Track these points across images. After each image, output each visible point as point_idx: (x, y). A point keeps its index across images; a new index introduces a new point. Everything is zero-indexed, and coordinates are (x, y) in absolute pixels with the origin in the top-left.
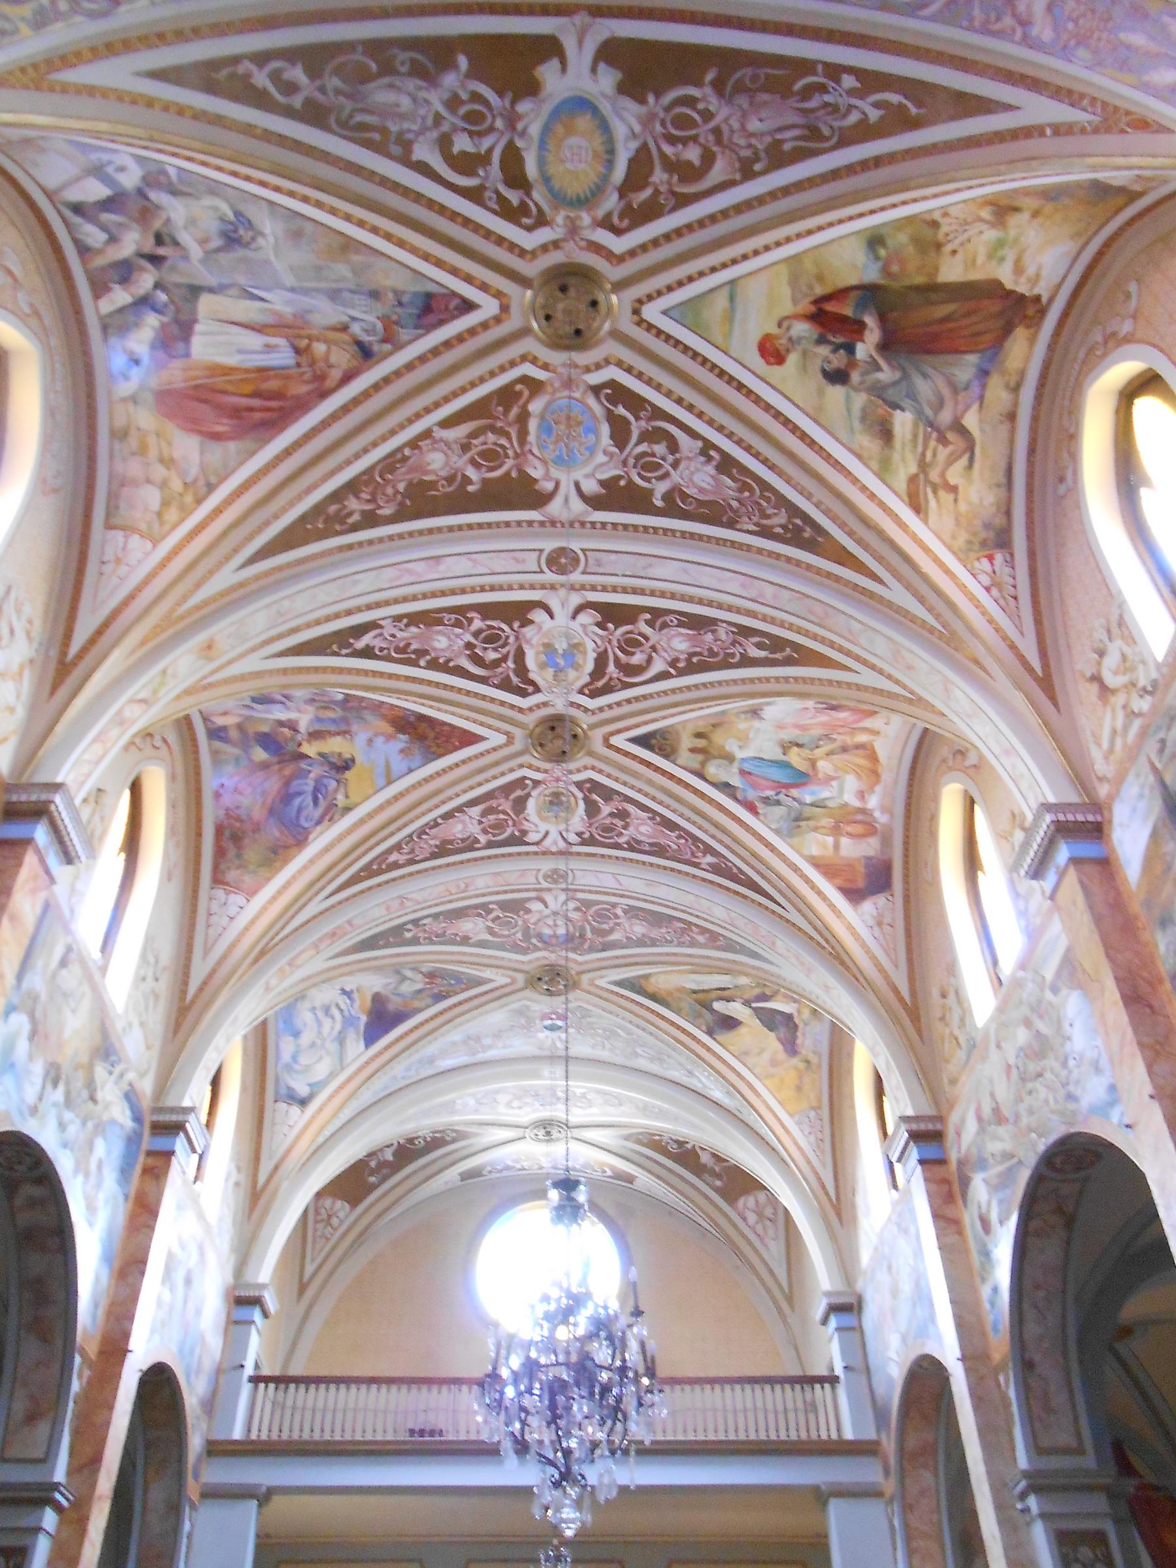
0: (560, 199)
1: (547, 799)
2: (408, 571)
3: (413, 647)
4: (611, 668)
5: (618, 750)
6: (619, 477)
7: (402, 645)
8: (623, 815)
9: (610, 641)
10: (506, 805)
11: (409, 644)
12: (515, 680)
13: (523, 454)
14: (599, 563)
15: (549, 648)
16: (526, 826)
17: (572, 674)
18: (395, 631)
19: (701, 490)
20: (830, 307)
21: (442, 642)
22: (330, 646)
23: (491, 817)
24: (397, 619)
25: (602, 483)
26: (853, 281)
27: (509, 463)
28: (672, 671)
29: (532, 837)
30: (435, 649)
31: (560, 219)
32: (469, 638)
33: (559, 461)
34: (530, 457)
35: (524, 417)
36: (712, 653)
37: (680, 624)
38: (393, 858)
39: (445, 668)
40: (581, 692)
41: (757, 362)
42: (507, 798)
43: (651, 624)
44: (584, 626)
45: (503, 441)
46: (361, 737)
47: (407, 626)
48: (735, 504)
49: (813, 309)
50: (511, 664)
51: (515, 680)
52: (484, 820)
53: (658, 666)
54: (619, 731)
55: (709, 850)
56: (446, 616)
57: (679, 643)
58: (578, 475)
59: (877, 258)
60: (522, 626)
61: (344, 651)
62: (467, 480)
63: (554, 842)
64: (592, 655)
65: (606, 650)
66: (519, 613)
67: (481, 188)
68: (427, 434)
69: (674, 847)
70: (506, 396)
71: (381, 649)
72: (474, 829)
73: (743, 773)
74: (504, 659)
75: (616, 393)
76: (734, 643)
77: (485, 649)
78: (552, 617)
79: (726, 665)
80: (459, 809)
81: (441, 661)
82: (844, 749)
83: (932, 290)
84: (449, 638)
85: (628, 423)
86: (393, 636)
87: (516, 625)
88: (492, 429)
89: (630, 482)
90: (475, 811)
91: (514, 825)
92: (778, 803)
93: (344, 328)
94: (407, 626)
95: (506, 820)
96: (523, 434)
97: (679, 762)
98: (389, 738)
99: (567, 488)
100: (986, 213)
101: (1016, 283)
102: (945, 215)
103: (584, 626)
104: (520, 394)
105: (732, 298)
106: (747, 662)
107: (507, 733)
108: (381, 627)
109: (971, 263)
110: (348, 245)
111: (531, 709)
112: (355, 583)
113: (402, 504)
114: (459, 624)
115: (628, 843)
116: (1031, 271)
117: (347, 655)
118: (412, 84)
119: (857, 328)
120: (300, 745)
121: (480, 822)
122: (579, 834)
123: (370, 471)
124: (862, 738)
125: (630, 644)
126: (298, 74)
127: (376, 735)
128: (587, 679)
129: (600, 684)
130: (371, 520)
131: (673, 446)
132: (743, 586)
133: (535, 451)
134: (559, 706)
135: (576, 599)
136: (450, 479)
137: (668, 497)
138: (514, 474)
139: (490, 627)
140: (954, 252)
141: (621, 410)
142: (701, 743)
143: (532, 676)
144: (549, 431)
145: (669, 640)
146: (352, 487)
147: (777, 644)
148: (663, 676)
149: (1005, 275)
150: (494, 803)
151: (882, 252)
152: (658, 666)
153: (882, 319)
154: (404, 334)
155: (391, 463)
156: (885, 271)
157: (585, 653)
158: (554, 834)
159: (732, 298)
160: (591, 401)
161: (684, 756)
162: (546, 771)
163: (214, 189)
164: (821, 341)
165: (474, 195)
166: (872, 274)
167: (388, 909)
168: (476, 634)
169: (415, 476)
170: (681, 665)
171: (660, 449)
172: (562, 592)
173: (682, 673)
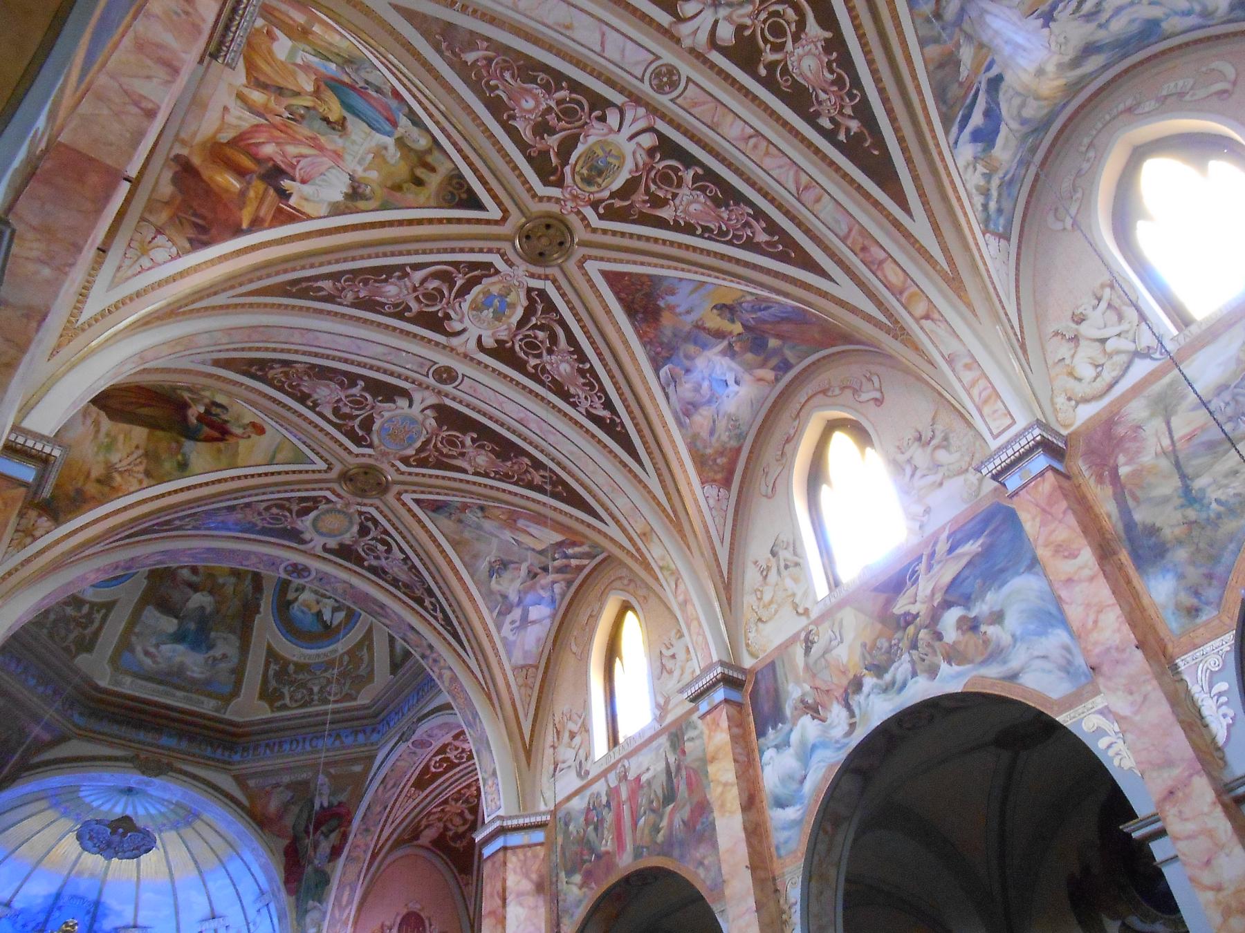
0: (350, 516)
1: (599, 180)
2: (541, 429)
3: (583, 381)
4: (459, 283)
5: (500, 204)
6: (380, 401)
8: (542, 129)
9: (448, 303)
10: (640, 196)
11: (584, 384)
12: (540, 307)
13: (432, 434)
14: (422, 365)
15: (498, 316)
16: (642, 158)
17: (495, 290)
18: (583, 400)
20: (216, 434)
21: (563, 367)
22: (619, 432)
23: (661, 194)
24: (574, 405)
25: (394, 402)
26: (200, 444)
27: (444, 434)
28: (408, 270)
29: (648, 140)
30: (572, 367)
31: (352, 510)
32: (546, 357)
34: (429, 431)
35: (419, 451)
36: (366, 282)
38: (762, 237)
40: (497, 272)
41: (267, 427)
42: (631, 206)
43: (408, 309)
44: (461, 321)
45: (439, 445)
46: (693, 317)
47: (573, 396)
49: (227, 437)
50: (534, 321)
51: (540, 307)
52: (669, 196)
53: (418, 276)
55: (463, 70)
56: (547, 381)
57: (392, 291)
58: (407, 410)
59: (184, 455)
60: (506, 342)
62: (473, 440)
63: (637, 118)
64: (469, 298)
65: (455, 298)
66: (502, 352)
67: (382, 533)
68: (476, 474)
69: (507, 75)
70: (423, 463)
71: (600, 398)
72: (685, 193)
73: (395, 124)
74: (535, 327)
77: (541, 342)
79: (355, 273)
80: (676, 227)
81: (576, 357)
82: (280, 91)
83: (151, 424)
84: (558, 367)
86: (586, 398)
87: (509, 345)
88: (441, 453)
90: (666, 213)
91: (653, 168)
92: (367, 82)
93: (485, 517)
94: (573, 396)
95: (654, 182)
97: (450, 166)
98: (671, 308)
99: (417, 407)
100: (118, 478)
101: (98, 414)
102: (141, 482)
103: (461, 321)
105: (273, 457)
106: (335, 276)
108: (587, 411)
109: (127, 435)
110: (455, 544)
112: (572, 453)
113: (516, 456)
114: (544, 370)
115: (560, 88)
116: (89, 421)
117: (619, 417)
118: (390, 571)
119: (200, 418)
120: (739, 334)
121: (675, 196)
122: (602, 119)
123: (516, 484)
124: (257, 96)
125: (432, 297)
126: (427, 603)
127: (680, 314)
128: (485, 281)
130: (538, 465)
133: (424, 432)
134: (522, 268)
135: (455, 342)
136: (482, 447)
138: (445, 428)
139: (525, 353)
140: (137, 447)
142: (421, 173)
143: (525, 303)
144: (410, 438)
145: (398, 295)
146: (530, 486)
148: (417, 267)
150: (646, 209)
151: (180, 457)
152: (418, 276)
153: (185, 418)
154: (458, 505)
155: (506, 477)
157: (473, 301)
158: (627, 131)
159: (273, 457)
160: (376, 441)
161: (444, 168)
162: (579, 213)
163: (488, 594)
164: (226, 422)
165: (386, 532)
166: (188, 445)
167: (818, 200)
168: (539, 356)
169: (498, 461)
173: (401, 267)
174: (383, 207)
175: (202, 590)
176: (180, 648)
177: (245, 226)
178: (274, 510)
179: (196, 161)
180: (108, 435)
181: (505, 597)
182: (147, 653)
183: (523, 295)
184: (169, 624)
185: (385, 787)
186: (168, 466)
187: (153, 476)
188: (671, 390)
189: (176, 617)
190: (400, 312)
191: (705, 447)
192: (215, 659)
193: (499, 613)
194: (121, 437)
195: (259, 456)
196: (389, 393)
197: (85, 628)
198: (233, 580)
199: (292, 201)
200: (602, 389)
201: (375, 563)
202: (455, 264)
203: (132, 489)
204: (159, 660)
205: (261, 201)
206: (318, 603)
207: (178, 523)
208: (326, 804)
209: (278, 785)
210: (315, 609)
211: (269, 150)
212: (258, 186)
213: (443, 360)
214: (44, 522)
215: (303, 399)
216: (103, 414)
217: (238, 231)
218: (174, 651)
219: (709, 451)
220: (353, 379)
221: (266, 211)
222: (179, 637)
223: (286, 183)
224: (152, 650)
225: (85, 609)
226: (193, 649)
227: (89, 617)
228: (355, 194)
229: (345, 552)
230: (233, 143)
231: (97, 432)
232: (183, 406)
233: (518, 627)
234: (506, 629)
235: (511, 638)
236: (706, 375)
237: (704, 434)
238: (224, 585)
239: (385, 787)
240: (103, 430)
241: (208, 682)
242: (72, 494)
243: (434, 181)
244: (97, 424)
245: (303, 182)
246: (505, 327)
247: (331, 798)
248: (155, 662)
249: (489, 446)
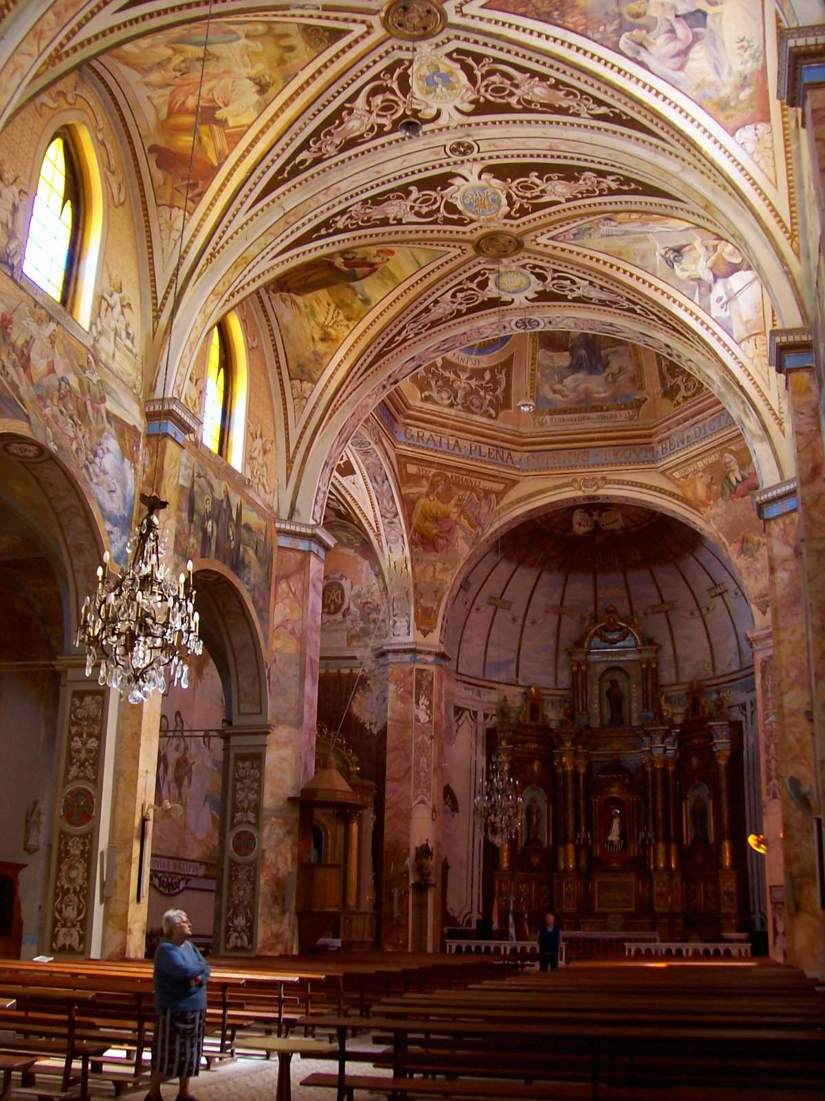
3: (562, 93)
4: (395, 86)
7: (571, 97)
9: (405, 103)
12: (470, 61)
17: (425, 72)
19: (392, 205)
20: (367, 269)
21: (539, 92)
24: (576, 115)
28: (348, 105)
33: (483, 189)
36: (329, 133)
37: (361, 136)
39: (534, 74)
43: (381, 126)
44: (428, 106)
45: (520, 194)
48: (368, 211)
50: (479, 74)
51: (470, 61)
53: (360, 102)
54: (363, 37)
57: (354, 125)
61: (618, 111)
62: (539, 177)
66: (481, 108)
68: (568, 200)
74: (484, 77)
75: (461, 222)
76: (320, 149)
77: (501, 83)
78: (456, 108)
79: (316, 133)
83: (325, 284)
84: (533, 93)
85: (448, 213)
89: (435, 190)
96: (509, 197)
99: (473, 179)
102: (347, 326)
104: (515, 213)
106: (305, 146)
107: (464, 15)
109: (318, 300)
111: (449, 40)
112: (609, 155)
124: (155, 77)
125: (388, 107)
129: (398, 72)
130: (602, 174)
131: (418, 214)
132: (339, 189)
134: (425, 47)
135: (443, 121)
137: (409, 193)
138: (509, 180)
139: (502, 98)
141: (455, 217)
142: (284, 42)
145: (362, 124)
147: (295, 172)
149: (300, 300)
153: (339, 271)
155: (590, 193)
156: (355, 293)
157: (421, 90)
160: (474, 217)
170: (344, 113)
171: (424, 210)
172: (453, 124)
173: (341, 108)
174: (287, 82)
177: (216, 164)
178: (459, 295)
179: (161, 143)
180: (306, 306)
181: (699, 280)
182: (555, 391)
183: (448, 61)
186: (357, 305)
187: (353, 318)
188: (644, 56)
190: (380, 132)
191: (718, 90)
192: (613, 375)
193: (701, 296)
194: (314, 303)
195: (410, 269)
196: (443, 181)
197: (495, 390)
199: (231, 123)
200: (582, 93)
201: (575, 295)
202: (376, 77)
203: (346, 335)
204: (567, 393)
205: (213, 137)
207: (399, 338)
208: (740, 479)
209: (696, 472)
211: (191, 102)
212: (204, 129)
213: (449, 139)
214: (307, 385)
215: (385, 222)
216: (292, 294)
217: (215, 170)
218: (576, 381)
219: (725, 92)
220: (404, 191)
221: (221, 143)
222: (576, 367)
223: (219, 115)
224: (558, 386)
225: (487, 376)
226: (591, 373)
227: (494, 380)
228: (263, 88)
229: (543, 296)
230: (171, 113)
231: (299, 308)
232: (331, 265)
233: (727, 303)
234: (716, 310)
235: (723, 314)
236: (671, 17)
237: (711, 77)
240: (301, 305)
241: (614, 398)
242: (312, 358)
243: (298, 41)
244: (294, 302)
245: (226, 105)
246: (464, 90)
248: (563, 396)
249: (555, 176)
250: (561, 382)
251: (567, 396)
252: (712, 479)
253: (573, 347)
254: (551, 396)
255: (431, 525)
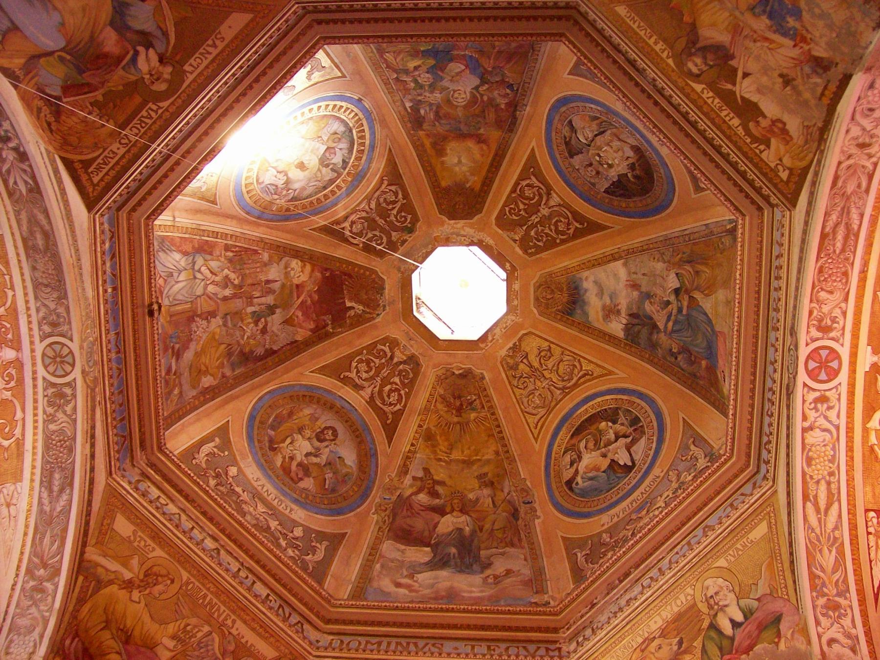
175: (453, 510)
176: (444, 573)
182: (398, 585)
184: (422, 555)
185: (816, 505)
189: (428, 545)
192: (496, 577)
198: (487, 491)
206: (604, 456)
208: (739, 617)
209: (649, 640)
210: (605, 464)
218: (436, 578)
222: (440, 562)
226: (461, 571)
238: (477, 499)
239: (816, 505)
247: (743, 602)
248: (411, 591)
250: (411, 576)
251: (417, 591)
252: (680, 643)
253: (437, 545)
254: (392, 588)
255: (112, 643)
